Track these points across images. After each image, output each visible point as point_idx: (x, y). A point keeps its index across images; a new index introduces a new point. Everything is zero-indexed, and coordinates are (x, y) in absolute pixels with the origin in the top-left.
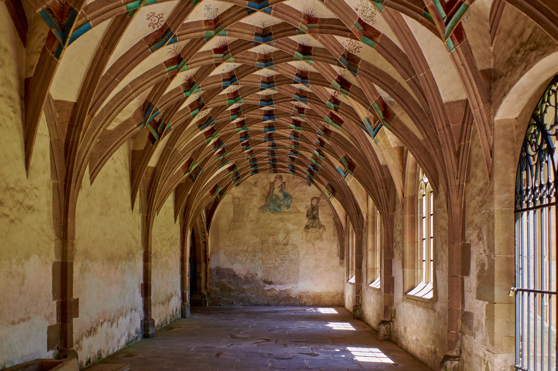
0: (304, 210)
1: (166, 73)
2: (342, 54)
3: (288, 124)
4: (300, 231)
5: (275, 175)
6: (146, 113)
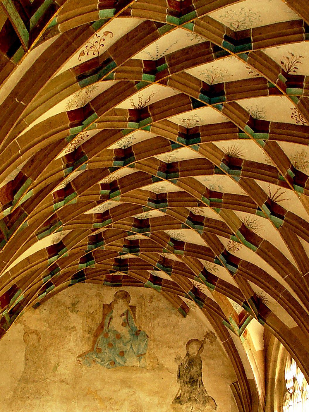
5: (114, 291)
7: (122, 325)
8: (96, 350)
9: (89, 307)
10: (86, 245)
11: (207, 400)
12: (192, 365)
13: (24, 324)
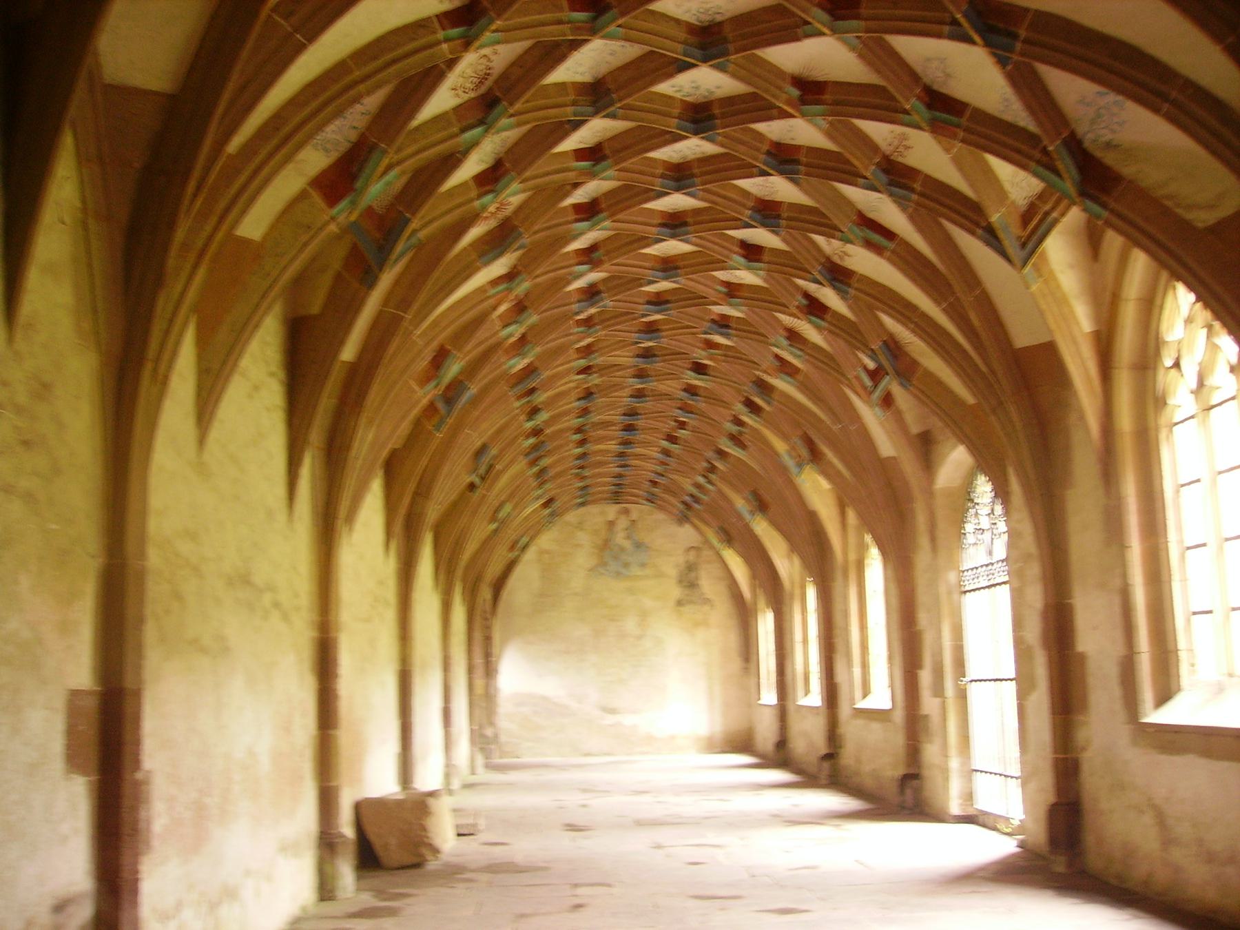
0: (672, 572)
8: (603, 564)
11: (707, 601)
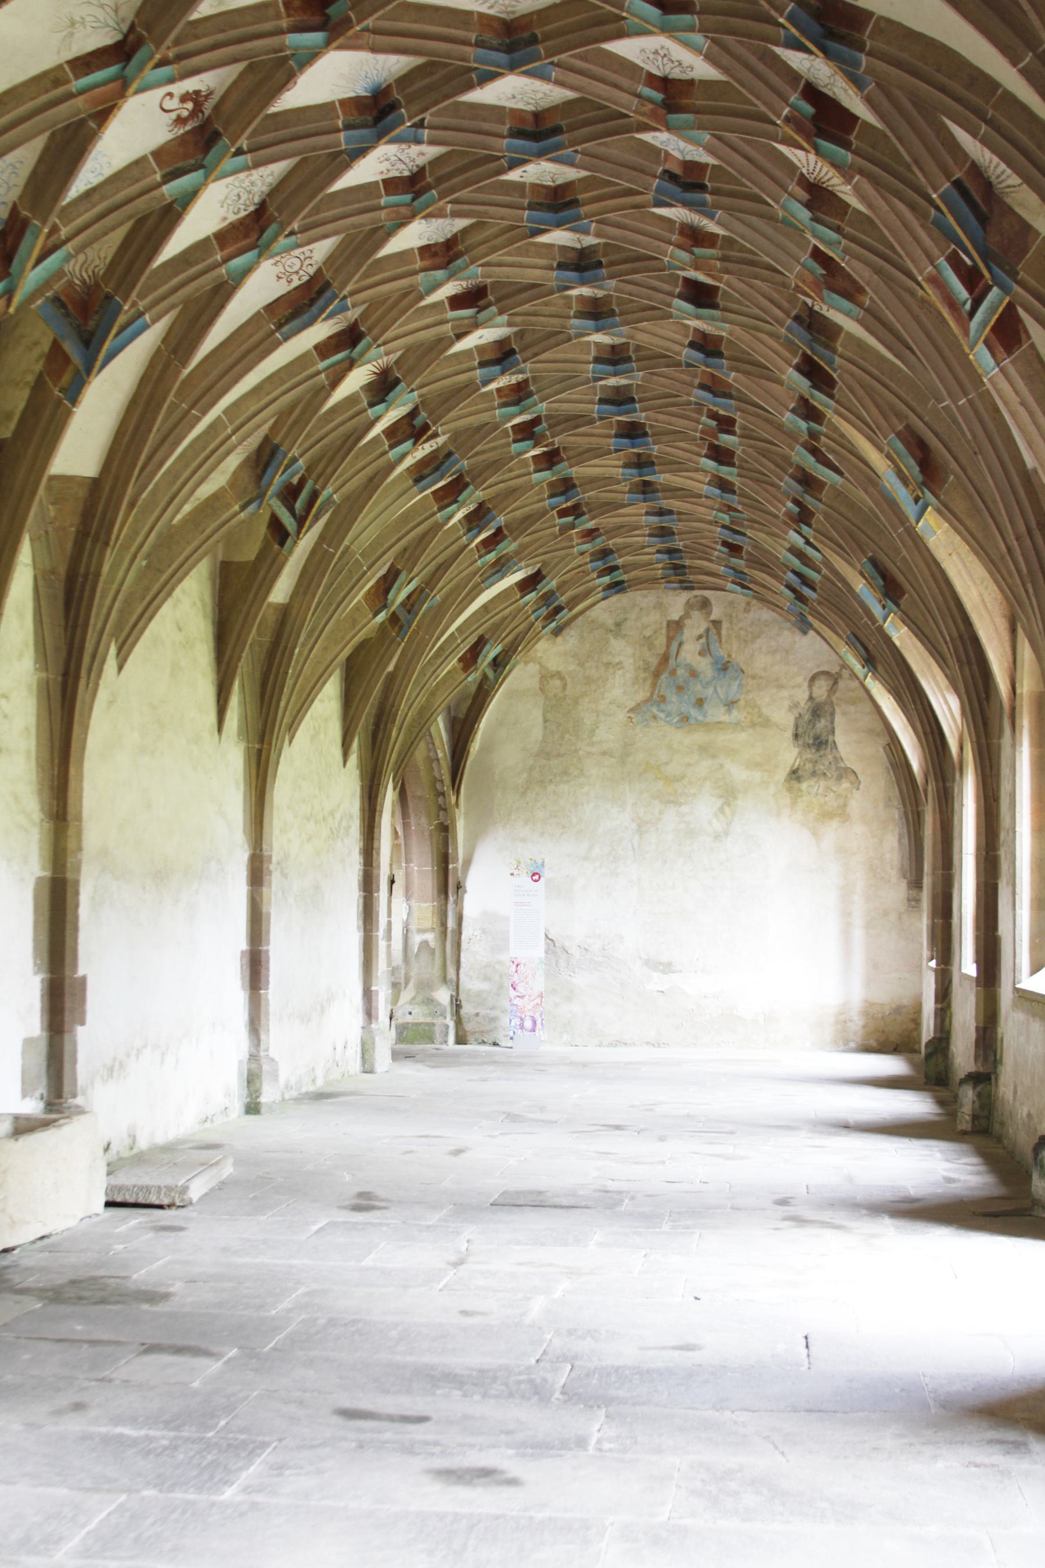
0: (783, 717)
1: (319, 373)
2: (794, 313)
3: (695, 458)
4: (772, 789)
5: (684, 596)
6: (264, 471)
7: (700, 654)
9: (644, 627)
10: (587, 564)
11: (845, 773)
12: (819, 716)
13: (540, 663)
